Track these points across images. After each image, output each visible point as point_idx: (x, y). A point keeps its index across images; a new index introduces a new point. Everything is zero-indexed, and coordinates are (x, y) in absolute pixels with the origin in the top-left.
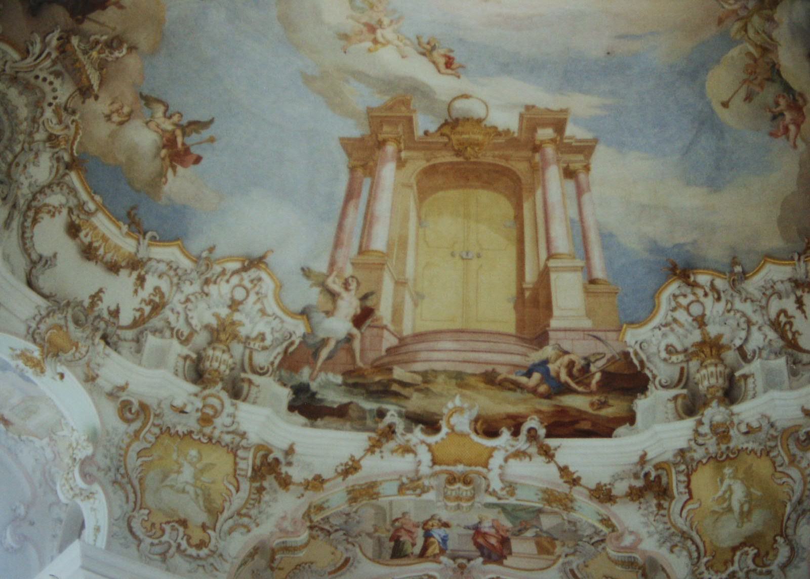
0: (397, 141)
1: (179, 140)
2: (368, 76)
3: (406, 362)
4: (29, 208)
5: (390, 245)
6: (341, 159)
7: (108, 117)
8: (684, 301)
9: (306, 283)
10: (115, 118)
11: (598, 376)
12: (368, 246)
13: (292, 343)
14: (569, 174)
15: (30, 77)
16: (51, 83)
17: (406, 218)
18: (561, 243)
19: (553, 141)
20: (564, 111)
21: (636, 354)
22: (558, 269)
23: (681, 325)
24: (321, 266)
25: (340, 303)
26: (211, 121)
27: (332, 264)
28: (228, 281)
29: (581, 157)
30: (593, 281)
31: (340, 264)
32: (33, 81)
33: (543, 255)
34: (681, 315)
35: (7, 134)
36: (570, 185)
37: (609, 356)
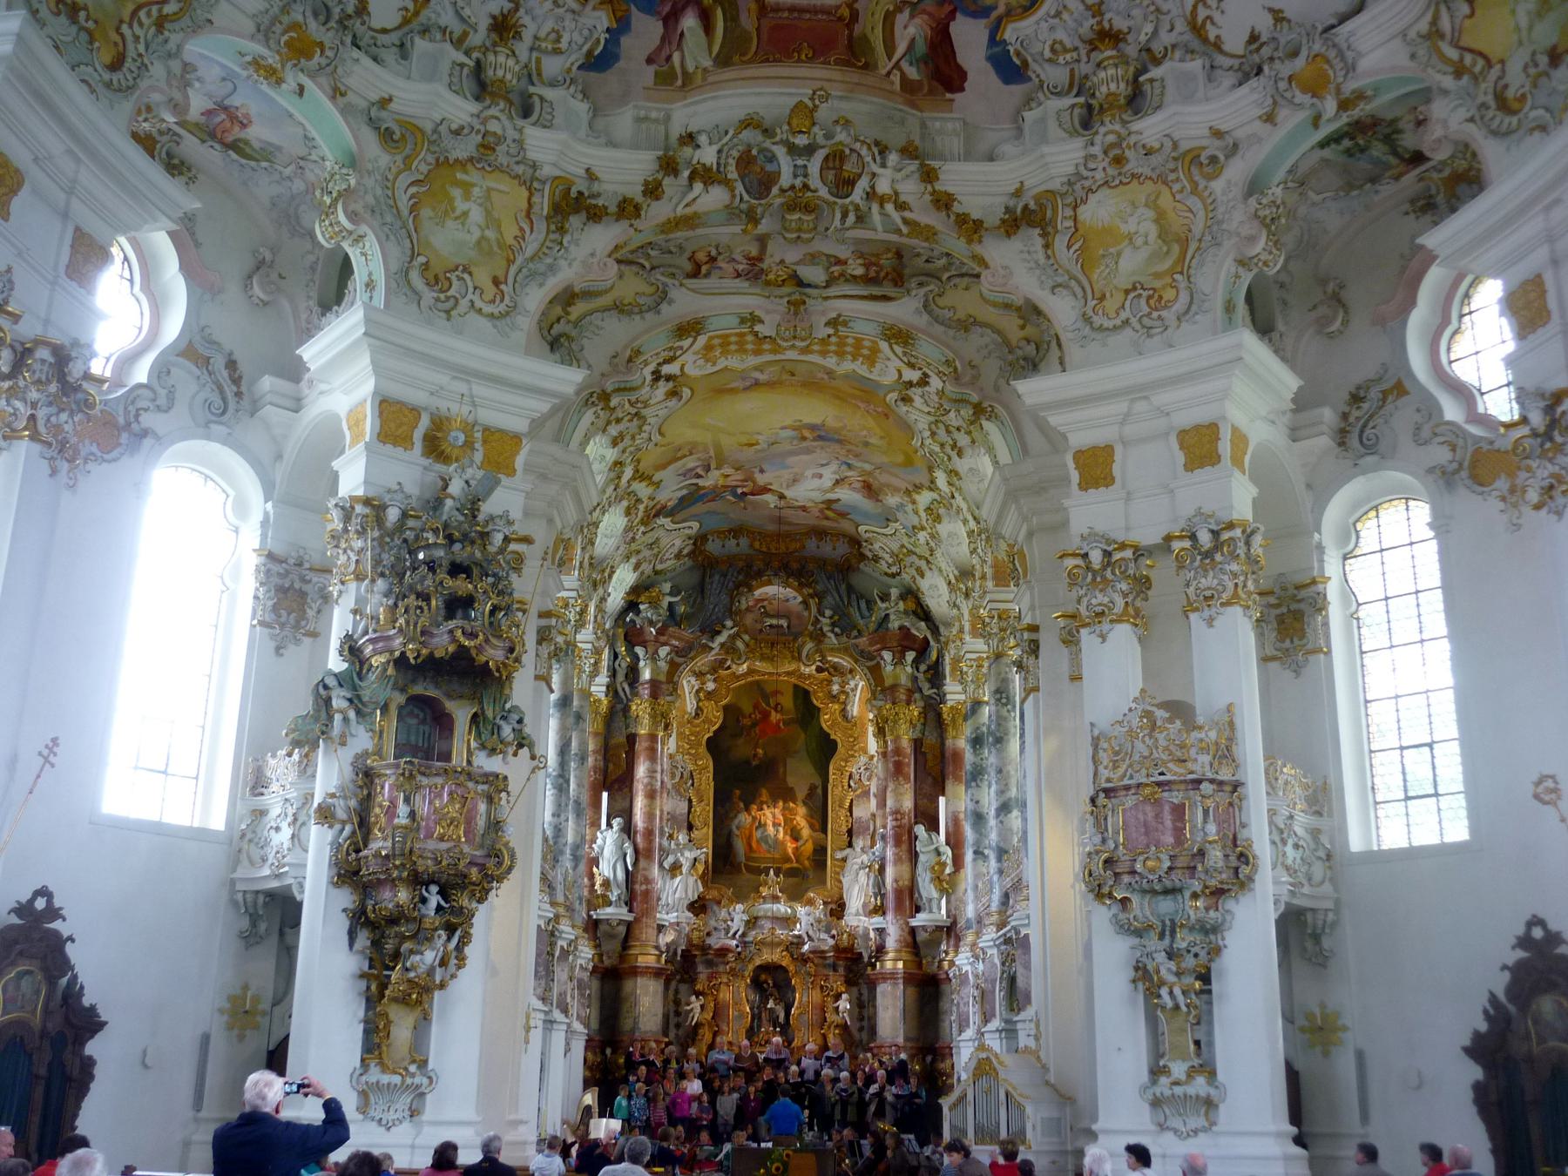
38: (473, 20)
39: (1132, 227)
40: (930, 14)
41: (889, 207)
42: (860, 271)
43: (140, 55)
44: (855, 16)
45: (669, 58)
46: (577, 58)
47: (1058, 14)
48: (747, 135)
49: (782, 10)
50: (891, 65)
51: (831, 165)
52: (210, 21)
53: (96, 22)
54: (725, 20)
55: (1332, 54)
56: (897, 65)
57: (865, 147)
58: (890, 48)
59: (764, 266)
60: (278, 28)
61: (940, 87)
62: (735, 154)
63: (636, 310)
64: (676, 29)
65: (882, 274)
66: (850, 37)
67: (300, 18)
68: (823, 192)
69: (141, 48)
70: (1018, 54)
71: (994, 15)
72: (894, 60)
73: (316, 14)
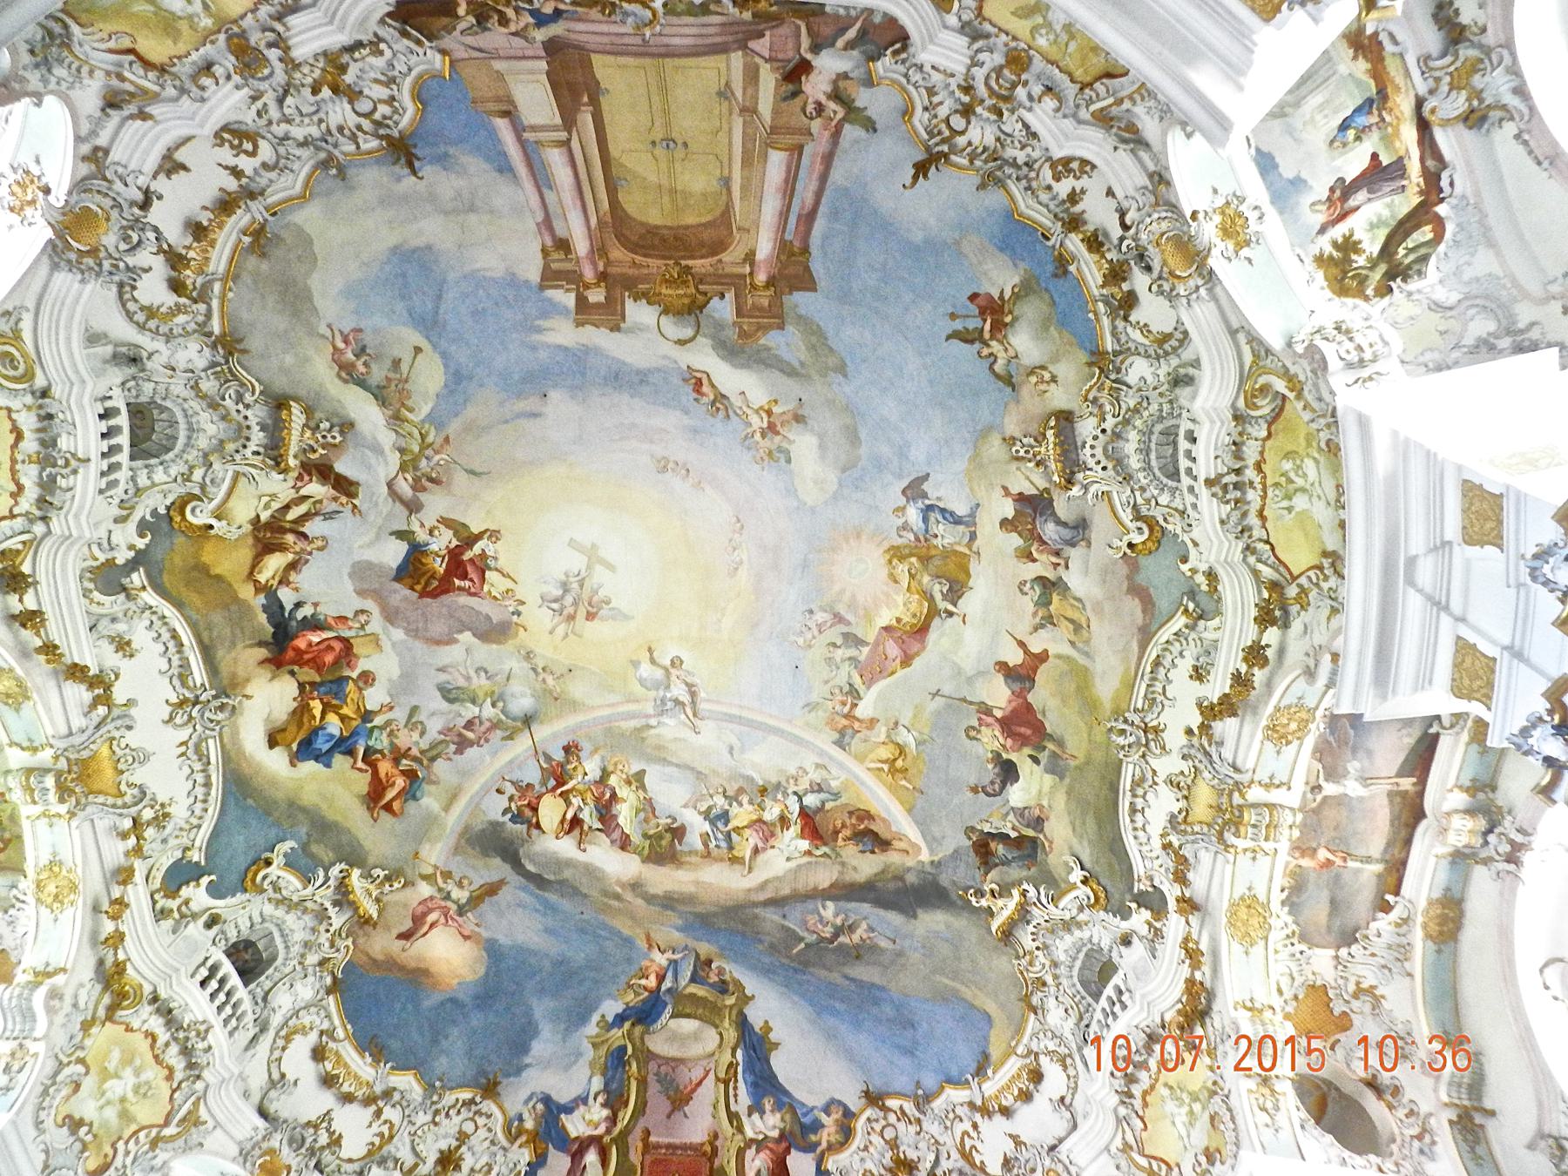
0: (754, 287)
1: (987, 327)
2: (782, 371)
3: (731, 24)
4: (1167, 354)
5: (765, 157)
6: (817, 266)
7: (1054, 379)
8: (383, 109)
9: (872, 113)
10: (1047, 376)
11: (461, 11)
12: (791, 155)
13: (896, 53)
14: (564, 245)
15: (1111, 472)
16: (1093, 456)
17: (745, 188)
18: (555, 159)
19: (587, 286)
20: (579, 324)
21: (419, 43)
22: (555, 128)
23: (376, 81)
24: (851, 132)
25: (829, 89)
26: (948, 338)
27: (837, 134)
28: (970, 144)
29: (554, 266)
30: (506, 114)
31: (827, 134)
32: (1110, 466)
33: (575, 144)
34: (380, 92)
35: (1158, 428)
36: (560, 232)
37: (456, 33)
38: (424, 1154)
43: (125, 1167)
44: (715, 1151)
47: (866, 1149)
52: (201, 1145)
53: (95, 1136)
55: (1060, 1168)
60: (257, 1152)
66: (711, 1168)
67: (277, 1145)
69: (129, 1161)
71: (819, 1150)
73: (291, 1141)
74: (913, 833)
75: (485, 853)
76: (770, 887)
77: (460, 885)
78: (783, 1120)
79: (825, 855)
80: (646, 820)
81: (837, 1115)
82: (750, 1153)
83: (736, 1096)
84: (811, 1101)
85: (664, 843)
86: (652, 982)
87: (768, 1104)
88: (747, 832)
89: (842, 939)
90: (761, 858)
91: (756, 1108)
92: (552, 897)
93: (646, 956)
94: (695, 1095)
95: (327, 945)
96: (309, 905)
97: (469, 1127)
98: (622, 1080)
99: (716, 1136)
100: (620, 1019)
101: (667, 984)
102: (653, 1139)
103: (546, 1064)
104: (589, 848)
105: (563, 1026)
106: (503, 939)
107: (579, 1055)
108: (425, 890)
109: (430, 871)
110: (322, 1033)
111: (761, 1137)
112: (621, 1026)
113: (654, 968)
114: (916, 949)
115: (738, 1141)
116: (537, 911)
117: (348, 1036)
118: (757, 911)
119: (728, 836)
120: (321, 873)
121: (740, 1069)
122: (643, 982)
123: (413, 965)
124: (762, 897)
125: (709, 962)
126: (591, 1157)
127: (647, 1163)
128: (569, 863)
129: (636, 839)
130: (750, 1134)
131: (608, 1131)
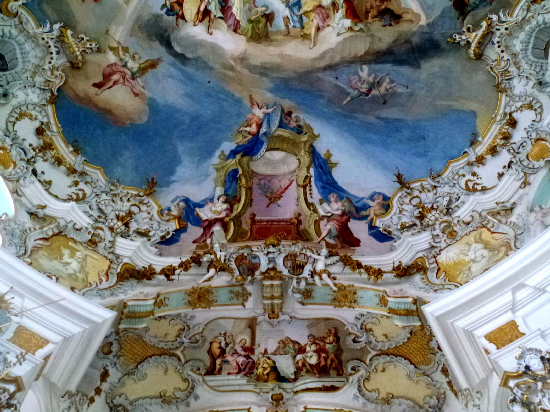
39: (472, 256)
40: (337, 220)
41: (325, 276)
42: (313, 360)
44: (300, 222)
45: (204, 241)
46: (156, 238)
47: (401, 212)
48: (241, 251)
49: (264, 221)
50: (320, 239)
51: (289, 258)
54: (234, 226)
56: (323, 239)
57: (308, 251)
58: (319, 233)
59: (254, 357)
61: (347, 246)
62: (234, 256)
63: (174, 401)
64: (209, 231)
65: (329, 362)
68: (286, 272)
70: (385, 230)
71: (369, 218)
72: (322, 237)
74: (415, 7)
75: (150, 37)
76: (328, 57)
77: (133, 58)
78: (343, 206)
79: (361, 30)
80: (250, 10)
81: (379, 200)
82: (323, 223)
83: (311, 194)
84: (361, 195)
85: (261, 25)
86: (254, 129)
87: (332, 197)
88: (312, 15)
89: (374, 92)
90: (322, 34)
91: (325, 200)
92: (190, 70)
93: (250, 112)
94: (283, 195)
95: (49, 73)
96: (41, 41)
97: (135, 209)
98: (235, 190)
99: (300, 215)
100: (234, 153)
101: (263, 130)
102: (257, 218)
103: (186, 181)
104: (215, 32)
105: (197, 159)
106: (160, 100)
107: (208, 175)
108: (112, 58)
109: (115, 45)
110: (42, 123)
111: (329, 215)
112: (234, 157)
113: (255, 119)
114: (421, 88)
115: (315, 217)
116: (182, 81)
117: (59, 132)
118: (320, 75)
119: (301, 18)
120: (48, 25)
121: (313, 179)
122: (248, 129)
123: (101, 105)
124: (322, 64)
125: (290, 114)
126: (217, 228)
127: (254, 231)
128: (200, 44)
129: (244, 24)
130: (322, 213)
131: (227, 215)
